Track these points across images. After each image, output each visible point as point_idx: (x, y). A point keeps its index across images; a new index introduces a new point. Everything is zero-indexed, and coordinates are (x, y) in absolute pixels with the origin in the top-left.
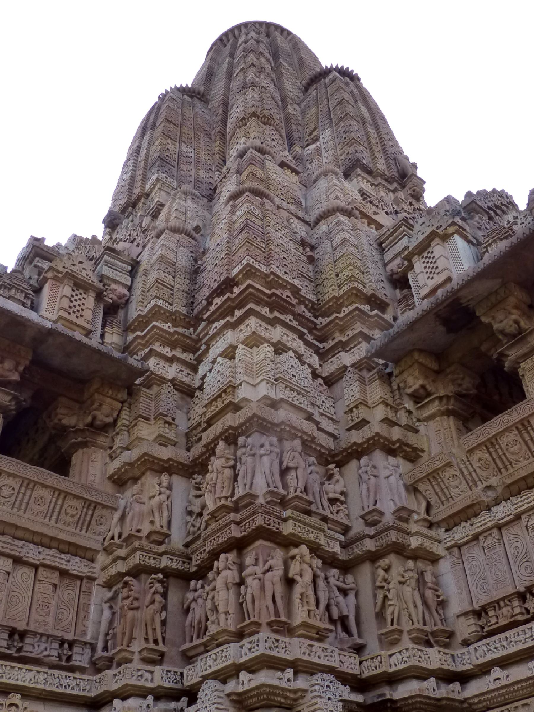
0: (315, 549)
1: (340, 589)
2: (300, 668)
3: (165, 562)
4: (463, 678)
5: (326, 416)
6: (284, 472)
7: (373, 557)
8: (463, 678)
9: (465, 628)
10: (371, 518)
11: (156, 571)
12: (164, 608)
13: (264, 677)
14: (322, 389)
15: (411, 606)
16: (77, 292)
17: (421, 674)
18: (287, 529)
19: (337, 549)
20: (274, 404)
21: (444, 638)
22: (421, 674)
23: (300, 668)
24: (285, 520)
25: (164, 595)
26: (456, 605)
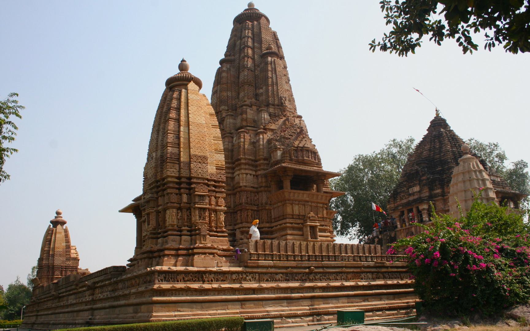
0: (252, 210)
4: (272, 227)
6: (247, 198)
7: (262, 210)
8: (272, 227)
9: (273, 221)
10: (262, 204)
13: (244, 229)
17: (266, 227)
18: (248, 208)
20: (246, 186)
21: (271, 222)
22: (266, 227)
26: (273, 217)
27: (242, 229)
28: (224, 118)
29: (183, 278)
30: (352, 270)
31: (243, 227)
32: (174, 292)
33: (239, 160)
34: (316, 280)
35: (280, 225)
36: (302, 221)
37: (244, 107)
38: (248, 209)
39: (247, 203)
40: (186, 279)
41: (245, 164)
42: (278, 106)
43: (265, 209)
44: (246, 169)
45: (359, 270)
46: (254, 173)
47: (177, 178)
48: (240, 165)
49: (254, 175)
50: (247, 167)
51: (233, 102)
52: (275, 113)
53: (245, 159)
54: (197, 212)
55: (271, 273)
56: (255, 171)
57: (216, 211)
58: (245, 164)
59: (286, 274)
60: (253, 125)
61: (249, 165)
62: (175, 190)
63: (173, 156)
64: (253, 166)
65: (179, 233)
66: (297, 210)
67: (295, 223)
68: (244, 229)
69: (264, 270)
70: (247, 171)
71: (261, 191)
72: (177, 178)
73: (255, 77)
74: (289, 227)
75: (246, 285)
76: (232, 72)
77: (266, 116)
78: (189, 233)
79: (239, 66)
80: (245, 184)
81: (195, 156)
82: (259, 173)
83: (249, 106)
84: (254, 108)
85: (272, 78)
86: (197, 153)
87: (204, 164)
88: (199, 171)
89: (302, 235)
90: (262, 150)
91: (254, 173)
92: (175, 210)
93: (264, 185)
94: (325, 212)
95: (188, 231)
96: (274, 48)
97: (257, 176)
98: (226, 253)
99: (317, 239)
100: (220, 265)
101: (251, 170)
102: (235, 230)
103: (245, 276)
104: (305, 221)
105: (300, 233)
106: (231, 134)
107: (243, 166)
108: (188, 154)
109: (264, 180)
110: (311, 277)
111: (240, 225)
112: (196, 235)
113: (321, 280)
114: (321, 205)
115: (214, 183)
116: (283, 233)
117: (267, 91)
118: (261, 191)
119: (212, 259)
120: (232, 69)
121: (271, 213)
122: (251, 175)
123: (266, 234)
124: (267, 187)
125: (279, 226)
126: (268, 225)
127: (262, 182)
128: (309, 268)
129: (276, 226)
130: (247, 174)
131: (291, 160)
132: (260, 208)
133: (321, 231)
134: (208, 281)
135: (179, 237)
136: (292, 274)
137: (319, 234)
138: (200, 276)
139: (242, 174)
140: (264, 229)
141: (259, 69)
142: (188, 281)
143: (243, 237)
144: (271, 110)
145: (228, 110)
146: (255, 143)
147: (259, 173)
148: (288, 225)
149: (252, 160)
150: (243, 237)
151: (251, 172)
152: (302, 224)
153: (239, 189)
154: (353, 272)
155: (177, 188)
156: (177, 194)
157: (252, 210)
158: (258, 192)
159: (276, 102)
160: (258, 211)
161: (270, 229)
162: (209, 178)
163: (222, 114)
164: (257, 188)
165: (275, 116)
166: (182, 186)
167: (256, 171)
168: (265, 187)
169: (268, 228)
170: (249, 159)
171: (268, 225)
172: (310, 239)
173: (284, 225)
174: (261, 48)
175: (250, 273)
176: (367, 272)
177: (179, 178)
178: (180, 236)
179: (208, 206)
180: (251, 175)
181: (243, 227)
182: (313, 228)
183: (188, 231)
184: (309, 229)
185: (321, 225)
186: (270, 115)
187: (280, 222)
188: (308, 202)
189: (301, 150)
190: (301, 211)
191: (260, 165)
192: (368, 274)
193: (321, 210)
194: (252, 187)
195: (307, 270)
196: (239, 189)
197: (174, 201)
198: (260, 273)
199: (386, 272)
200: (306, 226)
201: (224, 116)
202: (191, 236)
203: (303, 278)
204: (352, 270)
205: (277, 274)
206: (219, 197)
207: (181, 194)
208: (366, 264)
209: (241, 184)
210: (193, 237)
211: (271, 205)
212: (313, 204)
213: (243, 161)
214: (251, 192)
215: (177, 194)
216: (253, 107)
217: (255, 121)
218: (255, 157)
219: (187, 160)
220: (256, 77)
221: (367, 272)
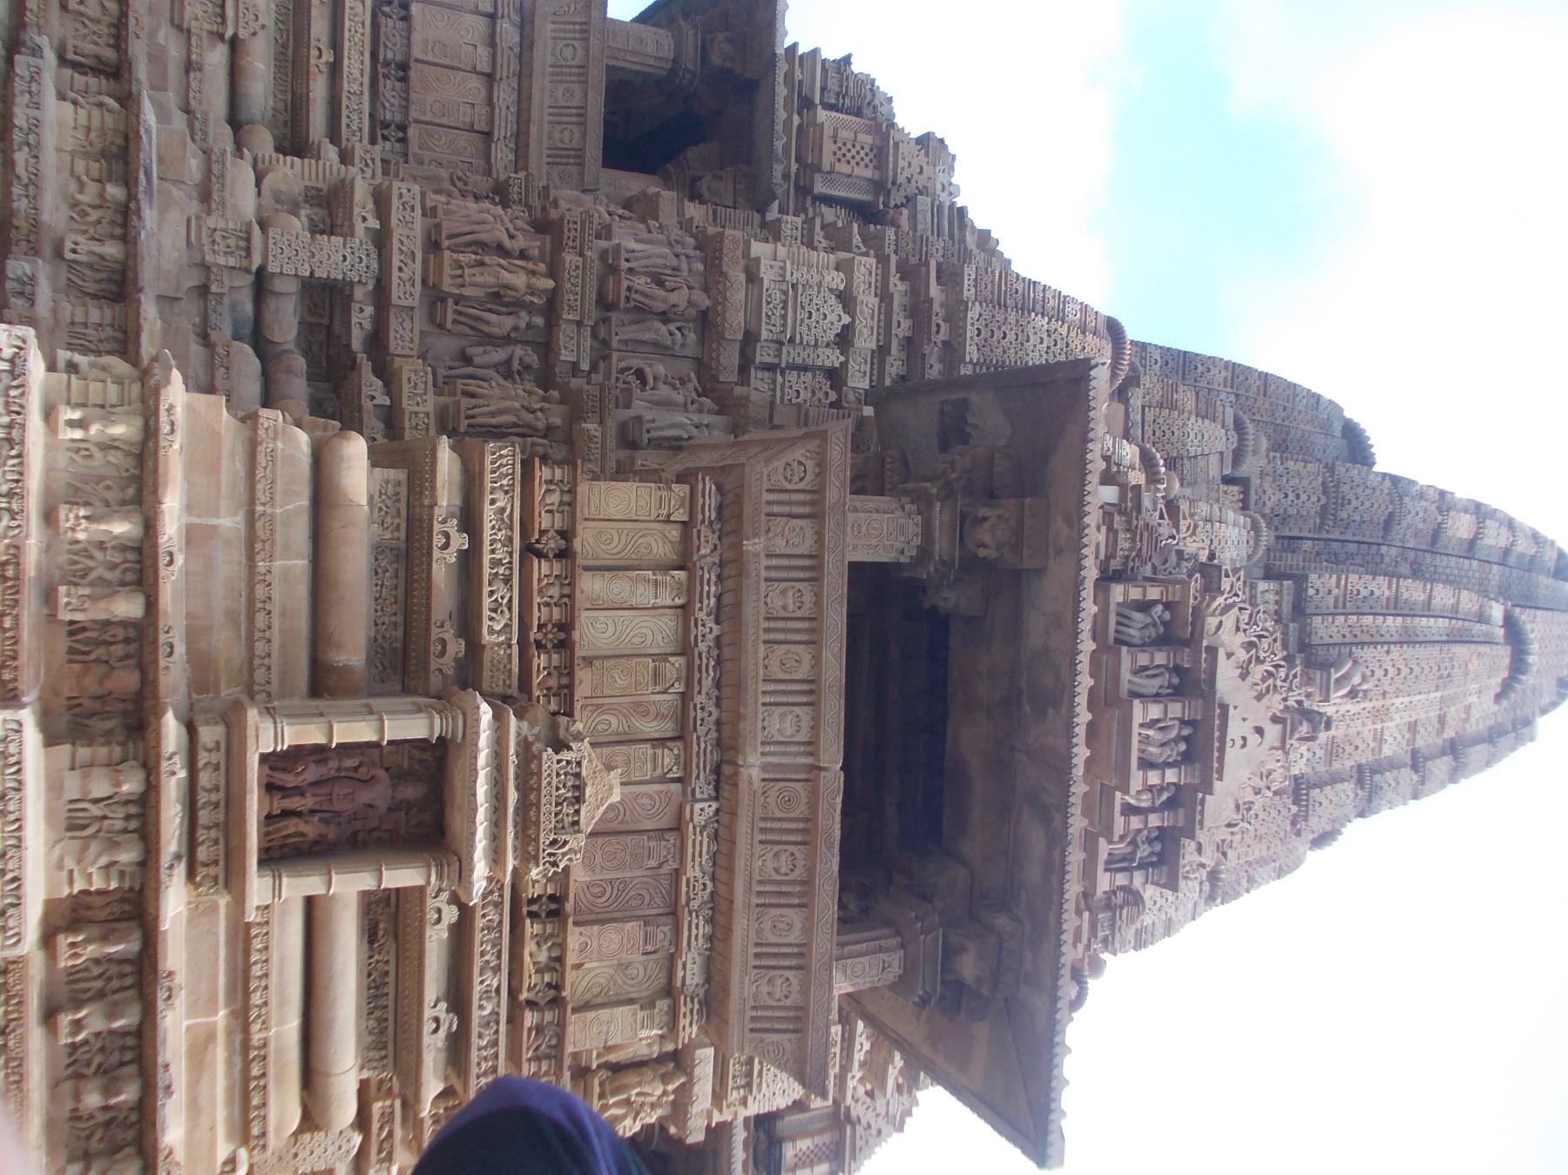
1: (508, 362)
5: (774, 390)
14: (821, 395)
15: (492, 408)
16: (871, 156)
18: (570, 259)
19: (567, 356)
20: (753, 277)
24: (581, 255)
67: (469, 561)
70: (868, 301)
74: (419, 480)
99: (277, 856)
114: (691, 972)
122: (844, 339)
133: (388, 920)
137: (348, 887)
172: (267, 735)
184: (408, 725)
185: (461, 934)
188: (723, 778)
190: (620, 680)
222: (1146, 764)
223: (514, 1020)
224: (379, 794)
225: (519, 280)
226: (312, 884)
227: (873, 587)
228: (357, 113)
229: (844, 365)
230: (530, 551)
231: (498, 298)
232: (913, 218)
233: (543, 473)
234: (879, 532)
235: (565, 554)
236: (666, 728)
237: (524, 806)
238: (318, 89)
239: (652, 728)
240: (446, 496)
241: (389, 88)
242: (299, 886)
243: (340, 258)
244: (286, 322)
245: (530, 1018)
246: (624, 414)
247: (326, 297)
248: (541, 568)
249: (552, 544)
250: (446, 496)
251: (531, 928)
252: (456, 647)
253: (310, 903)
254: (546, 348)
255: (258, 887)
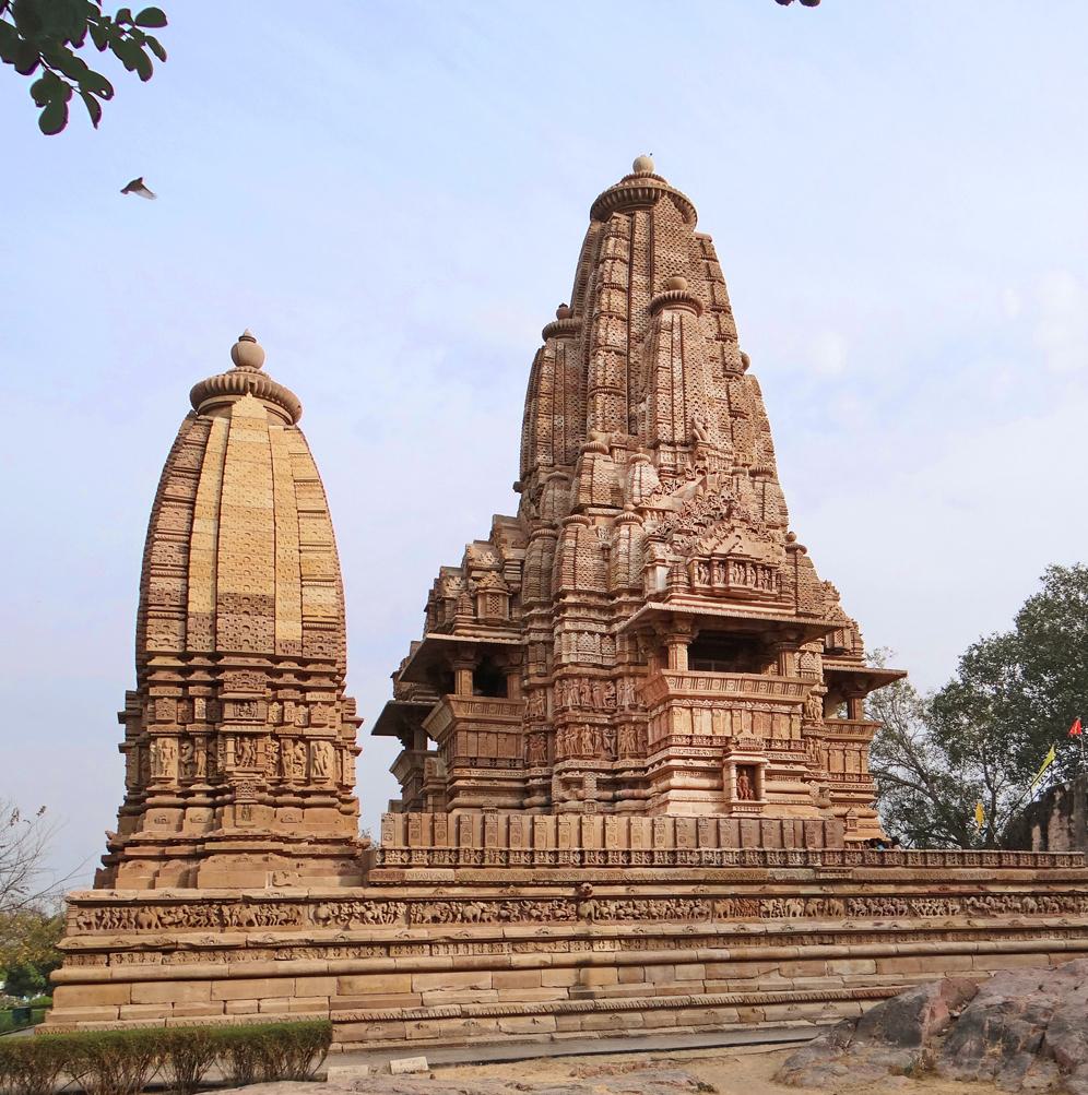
0: (592, 725)
2: (581, 770)
3: (544, 728)
4: (646, 770)
6: (581, 694)
9: (649, 751)
11: (541, 732)
12: (546, 746)
13: (569, 775)
17: (629, 769)
18: (580, 720)
19: (606, 722)
20: (577, 664)
22: (629, 769)
23: (581, 770)
25: (546, 741)
27: (564, 775)
28: (543, 485)
29: (160, 918)
30: (732, 890)
31: (567, 771)
32: (125, 955)
33: (564, 594)
34: (602, 916)
35: (659, 763)
36: (719, 753)
37: (586, 455)
38: (582, 724)
39: (580, 708)
40: (168, 919)
41: (577, 606)
42: (685, 445)
43: (630, 722)
44: (577, 619)
45: (755, 889)
46: (603, 629)
47: (210, 656)
48: (564, 608)
49: (603, 635)
50: (582, 613)
51: (569, 444)
52: (675, 466)
53: (578, 593)
54: (230, 744)
55: (448, 900)
56: (606, 622)
57: (302, 738)
58: (577, 606)
59: (501, 901)
60: (609, 503)
61: (589, 607)
62: (201, 688)
63: (167, 601)
64: (601, 609)
65: (181, 800)
66: (704, 724)
67: (695, 758)
68: (569, 775)
69: (428, 892)
70: (580, 625)
71: (621, 676)
72: (179, 657)
73: (629, 370)
74: (678, 769)
75: (359, 932)
76: (569, 363)
77: (649, 476)
78: (209, 800)
79: (588, 344)
80: (573, 659)
81: (233, 596)
82: (617, 627)
83: (604, 452)
84: (619, 455)
85: (671, 370)
86: (240, 590)
87: (261, 619)
88: (244, 637)
89: (720, 789)
90: (622, 568)
91: (603, 629)
92: (172, 744)
93: (628, 658)
94: (797, 727)
95: (209, 794)
96: (686, 287)
97: (613, 636)
98: (335, 849)
99: (757, 797)
100: (281, 880)
101: (594, 620)
102: (550, 777)
103: (359, 908)
104: (727, 752)
105: (715, 783)
106: (554, 527)
107: (569, 613)
108: (209, 593)
109: (627, 648)
110: (588, 907)
111: (560, 766)
112: (223, 804)
113: (619, 918)
115: (295, 666)
116: (663, 785)
117: (654, 407)
118: (621, 676)
119: (259, 867)
120: (570, 353)
121: (645, 731)
123: (631, 787)
124: (636, 664)
125: (657, 767)
126: (634, 763)
127: (622, 653)
128: (577, 885)
129: (653, 766)
130: (580, 632)
131: (692, 590)
132: (617, 720)
133: (770, 774)
134: (239, 924)
135: (181, 810)
136: (521, 900)
137: (764, 785)
138: (215, 910)
139: (567, 632)
140: (626, 774)
141: (640, 347)
142: (170, 924)
143: (566, 795)
144: (665, 457)
145: (552, 466)
146: (609, 549)
147: (617, 627)
148: (674, 762)
149: (601, 596)
150: (566, 795)
151: (593, 627)
152: (718, 759)
153: (558, 673)
154: (734, 896)
155: (179, 685)
156: (180, 700)
157: (591, 725)
158: (614, 679)
159: (680, 436)
160: (614, 727)
161: (639, 774)
162: (279, 653)
163: (537, 477)
164: (610, 668)
165: (676, 474)
166: (193, 677)
167: (609, 624)
168: (631, 664)
169: (635, 770)
170: (590, 593)
171: (634, 763)
172: (735, 799)
173: (665, 764)
174: (650, 288)
175: (378, 901)
176: (786, 896)
177: (185, 656)
178: (184, 806)
179: (268, 728)
180: (592, 633)
181: (567, 771)
182: (749, 770)
183: (209, 794)
184: (734, 773)
185: (772, 762)
186: (660, 474)
187: (659, 756)
189: (720, 562)
190: (717, 725)
191: (620, 606)
192: (789, 902)
193: (785, 720)
194: (595, 665)
195: (570, 892)
196: (558, 673)
197: (166, 718)
198: (408, 901)
199: (856, 896)
200: (728, 765)
201: (541, 481)
202: (213, 806)
203: (559, 913)
204: (732, 890)
205: (467, 901)
206: (316, 703)
207: (191, 700)
208: (781, 874)
209: (565, 660)
210: (218, 809)
211: (646, 710)
212: (761, 707)
213: (570, 599)
214: (592, 678)
215: (180, 700)
216: (616, 452)
217: (616, 491)
218: (607, 586)
219: (208, 609)
220: (630, 370)
221: (786, 896)
222: (745, 582)
223: (791, 751)
224: (746, 778)
225: (588, 735)
226: (763, 791)
227: (698, 659)
228: (519, 774)
229: (600, 634)
230: (691, 745)
231: (592, 740)
232: (514, 582)
233: (674, 742)
234: (681, 655)
235: (691, 737)
236: (728, 713)
237: (750, 750)
238: (505, 784)
239: (729, 717)
240: (681, 763)
241: (499, 764)
242: (763, 794)
243: (590, 781)
244: (609, 794)
245: (792, 748)
246: (627, 709)
247: (601, 785)
248: (695, 743)
249: (689, 740)
250: (681, 763)
251: (773, 747)
252: (713, 761)
253: (767, 792)
254: (605, 726)
255: (763, 801)
